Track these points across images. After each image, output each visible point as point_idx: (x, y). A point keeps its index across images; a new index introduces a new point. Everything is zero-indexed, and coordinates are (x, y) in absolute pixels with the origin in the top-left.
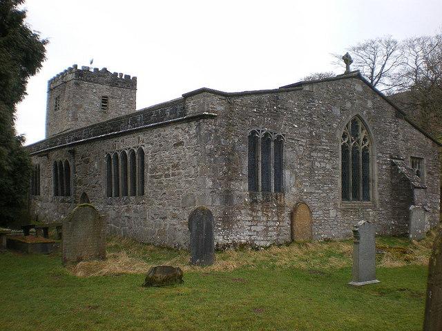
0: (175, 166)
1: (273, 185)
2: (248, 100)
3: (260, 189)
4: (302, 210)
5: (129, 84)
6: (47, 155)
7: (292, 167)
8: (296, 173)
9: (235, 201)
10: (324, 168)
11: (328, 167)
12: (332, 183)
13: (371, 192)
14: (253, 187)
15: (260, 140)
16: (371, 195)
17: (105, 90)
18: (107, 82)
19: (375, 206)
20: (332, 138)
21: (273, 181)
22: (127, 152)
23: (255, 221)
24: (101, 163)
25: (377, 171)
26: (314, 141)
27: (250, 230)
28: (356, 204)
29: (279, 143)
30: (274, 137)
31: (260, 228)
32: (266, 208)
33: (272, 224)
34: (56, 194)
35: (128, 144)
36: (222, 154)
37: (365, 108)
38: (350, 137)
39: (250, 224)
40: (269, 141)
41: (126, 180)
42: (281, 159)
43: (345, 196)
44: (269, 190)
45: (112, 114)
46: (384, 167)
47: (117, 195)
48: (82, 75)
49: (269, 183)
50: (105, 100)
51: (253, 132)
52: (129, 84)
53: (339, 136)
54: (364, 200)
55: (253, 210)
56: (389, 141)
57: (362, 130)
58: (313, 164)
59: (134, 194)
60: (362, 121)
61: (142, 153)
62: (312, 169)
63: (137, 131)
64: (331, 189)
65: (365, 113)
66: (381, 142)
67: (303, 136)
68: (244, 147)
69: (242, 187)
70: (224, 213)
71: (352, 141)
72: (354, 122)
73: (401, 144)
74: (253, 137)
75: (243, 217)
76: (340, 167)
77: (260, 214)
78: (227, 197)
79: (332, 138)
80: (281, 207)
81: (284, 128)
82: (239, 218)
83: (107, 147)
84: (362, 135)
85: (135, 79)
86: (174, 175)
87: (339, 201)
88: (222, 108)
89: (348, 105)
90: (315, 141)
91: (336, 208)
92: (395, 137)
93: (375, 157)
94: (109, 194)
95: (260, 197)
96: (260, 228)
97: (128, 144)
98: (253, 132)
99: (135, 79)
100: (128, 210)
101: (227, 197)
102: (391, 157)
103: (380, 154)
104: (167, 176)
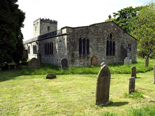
1: (86, 52)
2: (79, 29)
3: (82, 53)
4: (94, 58)
5: (55, 23)
6: (31, 43)
7: (92, 47)
8: (93, 49)
9: (75, 56)
10: (101, 47)
11: (102, 47)
12: (103, 51)
13: (115, 53)
14: (80, 53)
15: (82, 40)
16: (115, 54)
17: (48, 25)
18: (49, 23)
19: (116, 57)
20: (104, 39)
21: (86, 51)
22: (49, 43)
23: (81, 61)
24: (43, 46)
25: (117, 47)
26: (98, 40)
27: (79, 64)
28: (110, 57)
29: (88, 41)
30: (86, 39)
31: (82, 63)
32: (84, 57)
33: (86, 62)
34: (34, 54)
35: (49, 41)
36: (71, 44)
37: (114, 30)
38: (109, 38)
39: (79, 62)
40: (85, 40)
41: (49, 50)
42: (89, 45)
43: (107, 54)
44: (85, 53)
45: (51, 31)
46: (119, 46)
47: (47, 54)
48: (42, 21)
49: (85, 51)
50: (49, 28)
51: (81, 38)
52: (55, 23)
53: (106, 38)
54: (113, 55)
55: (80, 59)
56: (121, 39)
57: (113, 36)
58: (98, 46)
59: (51, 54)
60: (113, 34)
61: (52, 43)
62: (98, 47)
63: (52, 37)
64: (103, 53)
65: (114, 32)
66: (119, 40)
67: (95, 38)
68: (78, 42)
69: (77, 53)
70: (72, 59)
71: (110, 40)
72: (111, 34)
73: (125, 40)
75: (77, 61)
76: (106, 47)
77: (82, 59)
78: (73, 55)
79: (104, 39)
80: (88, 58)
81: (89, 36)
82: (76, 61)
84: (113, 39)
85: (57, 21)
87: (105, 56)
88: (71, 32)
89: (109, 30)
90: (99, 40)
91: (104, 58)
92: (123, 38)
93: (117, 44)
94: (45, 54)
95: (82, 55)
96: (82, 63)
97: (49, 41)
98: (81, 38)
99: (57, 21)
100: (50, 58)
101: (73, 55)
102: (122, 44)
103: (118, 43)
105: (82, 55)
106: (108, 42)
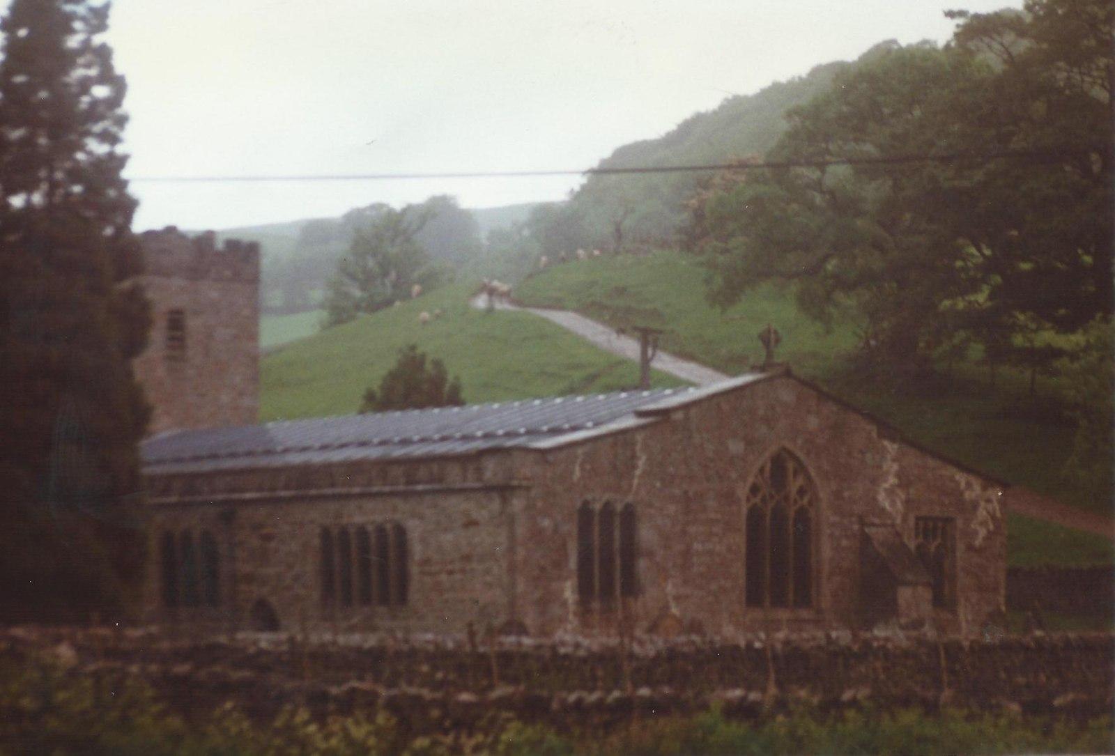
0: (467, 558)
14: (584, 589)
25: (830, 550)
30: (619, 507)
35: (367, 515)
53: (742, 491)
59: (384, 600)
61: (401, 531)
62: (687, 553)
63: (393, 494)
65: (800, 442)
69: (569, 592)
72: (778, 463)
74: (585, 513)
83: (317, 516)
84: (794, 485)
86: (463, 571)
95: (596, 605)
98: (586, 503)
104: (451, 573)
105: (596, 605)
106: (754, 517)
